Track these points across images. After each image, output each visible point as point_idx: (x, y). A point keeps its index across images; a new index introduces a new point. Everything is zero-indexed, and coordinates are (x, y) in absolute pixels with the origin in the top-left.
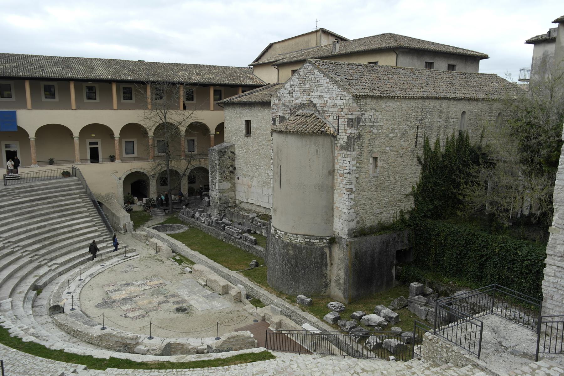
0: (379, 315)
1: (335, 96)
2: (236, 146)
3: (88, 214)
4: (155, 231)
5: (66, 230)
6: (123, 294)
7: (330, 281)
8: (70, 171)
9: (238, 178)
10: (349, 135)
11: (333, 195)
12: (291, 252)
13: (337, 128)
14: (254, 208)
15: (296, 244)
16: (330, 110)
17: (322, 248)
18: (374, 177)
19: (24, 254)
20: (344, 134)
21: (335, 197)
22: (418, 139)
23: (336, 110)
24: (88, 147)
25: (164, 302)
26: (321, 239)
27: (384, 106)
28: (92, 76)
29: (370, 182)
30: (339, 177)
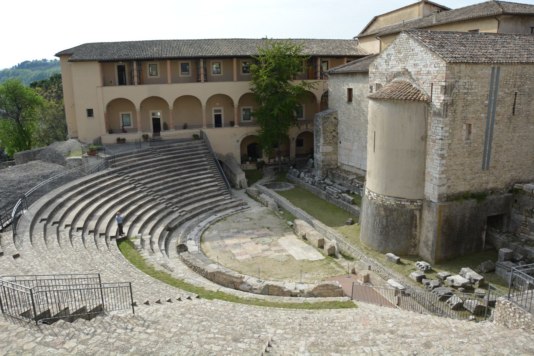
0: (465, 277)
1: (429, 64)
2: (339, 112)
3: (211, 171)
4: (264, 188)
5: (193, 183)
7: (419, 242)
8: (199, 134)
9: (340, 142)
10: (441, 101)
11: (425, 159)
12: (382, 213)
13: (430, 95)
14: (354, 170)
15: (387, 206)
17: (412, 210)
18: (466, 143)
19: (162, 201)
20: (437, 101)
21: (427, 162)
22: (516, 106)
24: (214, 114)
25: (267, 250)
26: (412, 202)
27: (479, 73)
28: (218, 54)
29: (463, 148)
30: (431, 143)
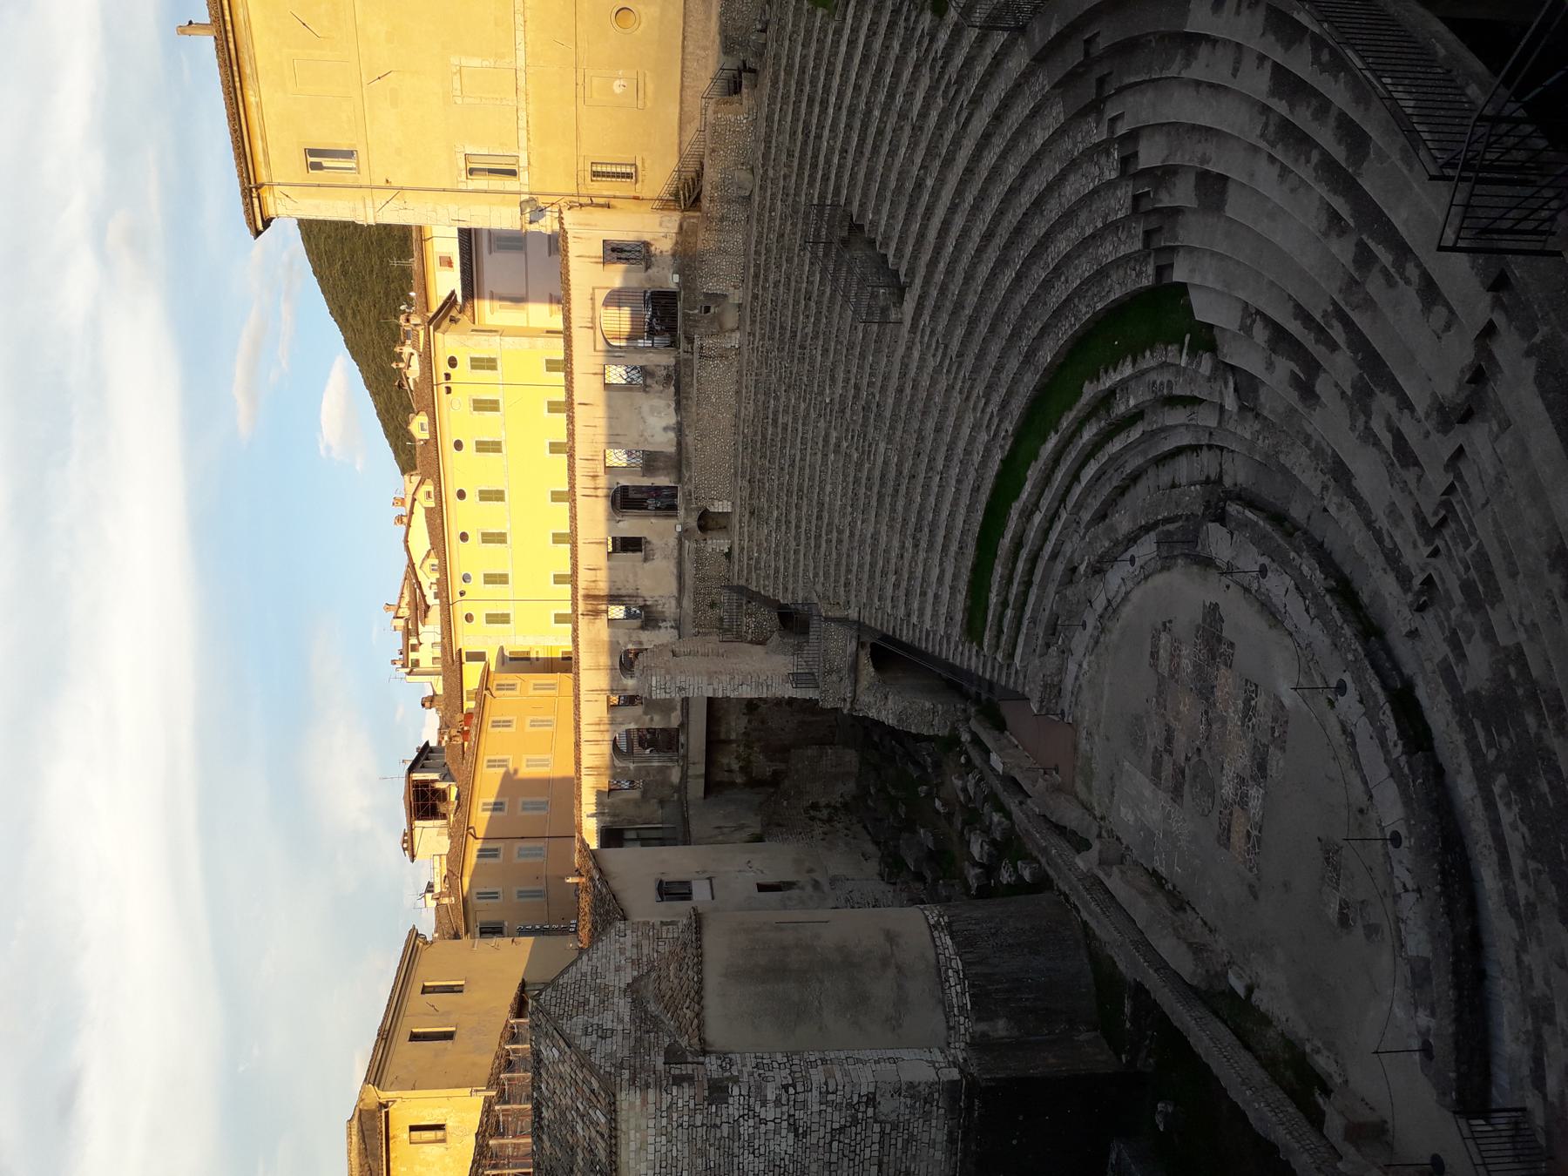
16: (645, 951)
23: (645, 942)
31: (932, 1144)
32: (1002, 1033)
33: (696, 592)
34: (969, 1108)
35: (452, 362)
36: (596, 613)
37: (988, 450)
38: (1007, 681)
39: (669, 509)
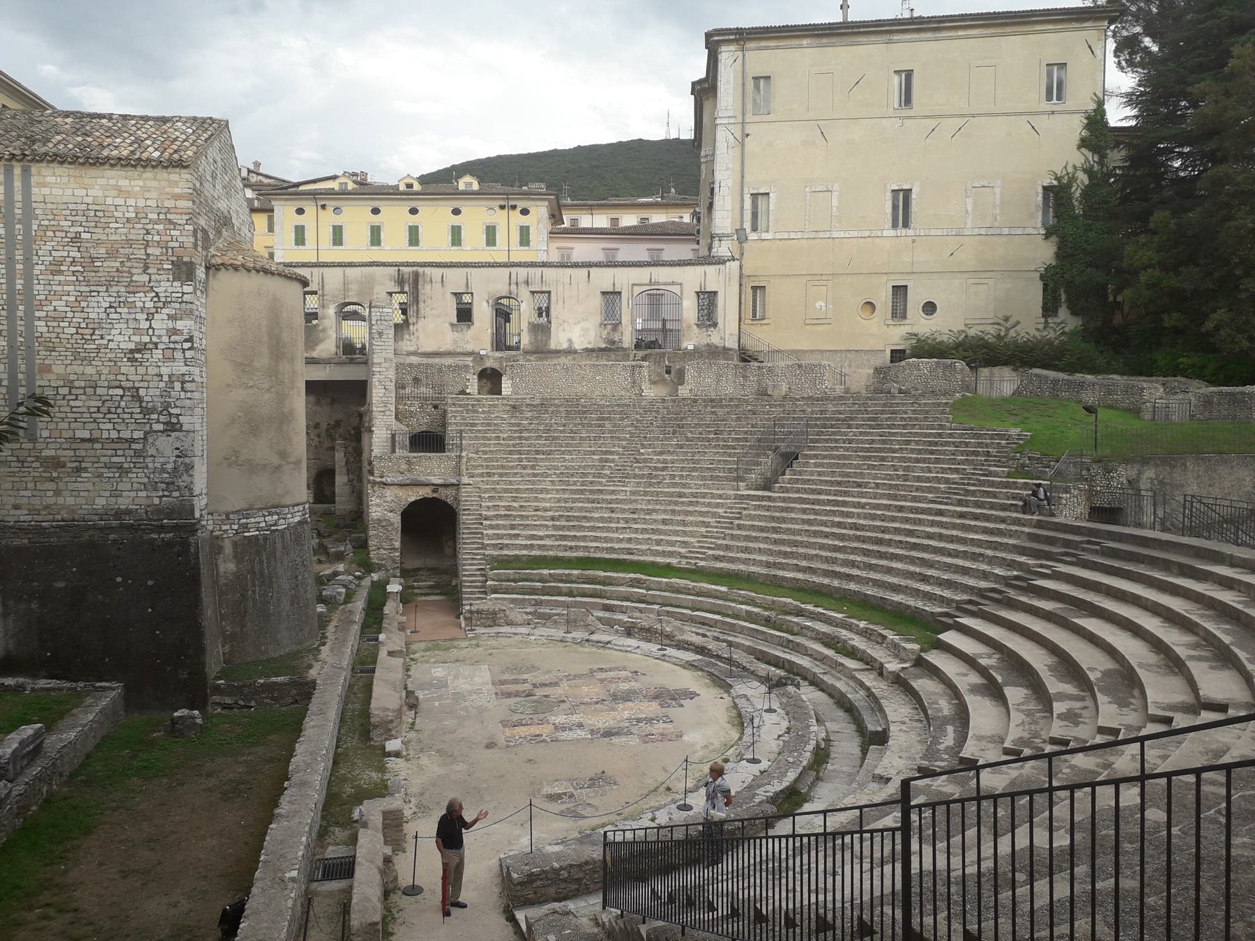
6: (626, 711)
31: (116, 494)
32: (222, 569)
33: (428, 366)
34: (162, 529)
35: (525, 212)
36: (400, 281)
37: (671, 554)
38: (467, 593)
39: (500, 343)
